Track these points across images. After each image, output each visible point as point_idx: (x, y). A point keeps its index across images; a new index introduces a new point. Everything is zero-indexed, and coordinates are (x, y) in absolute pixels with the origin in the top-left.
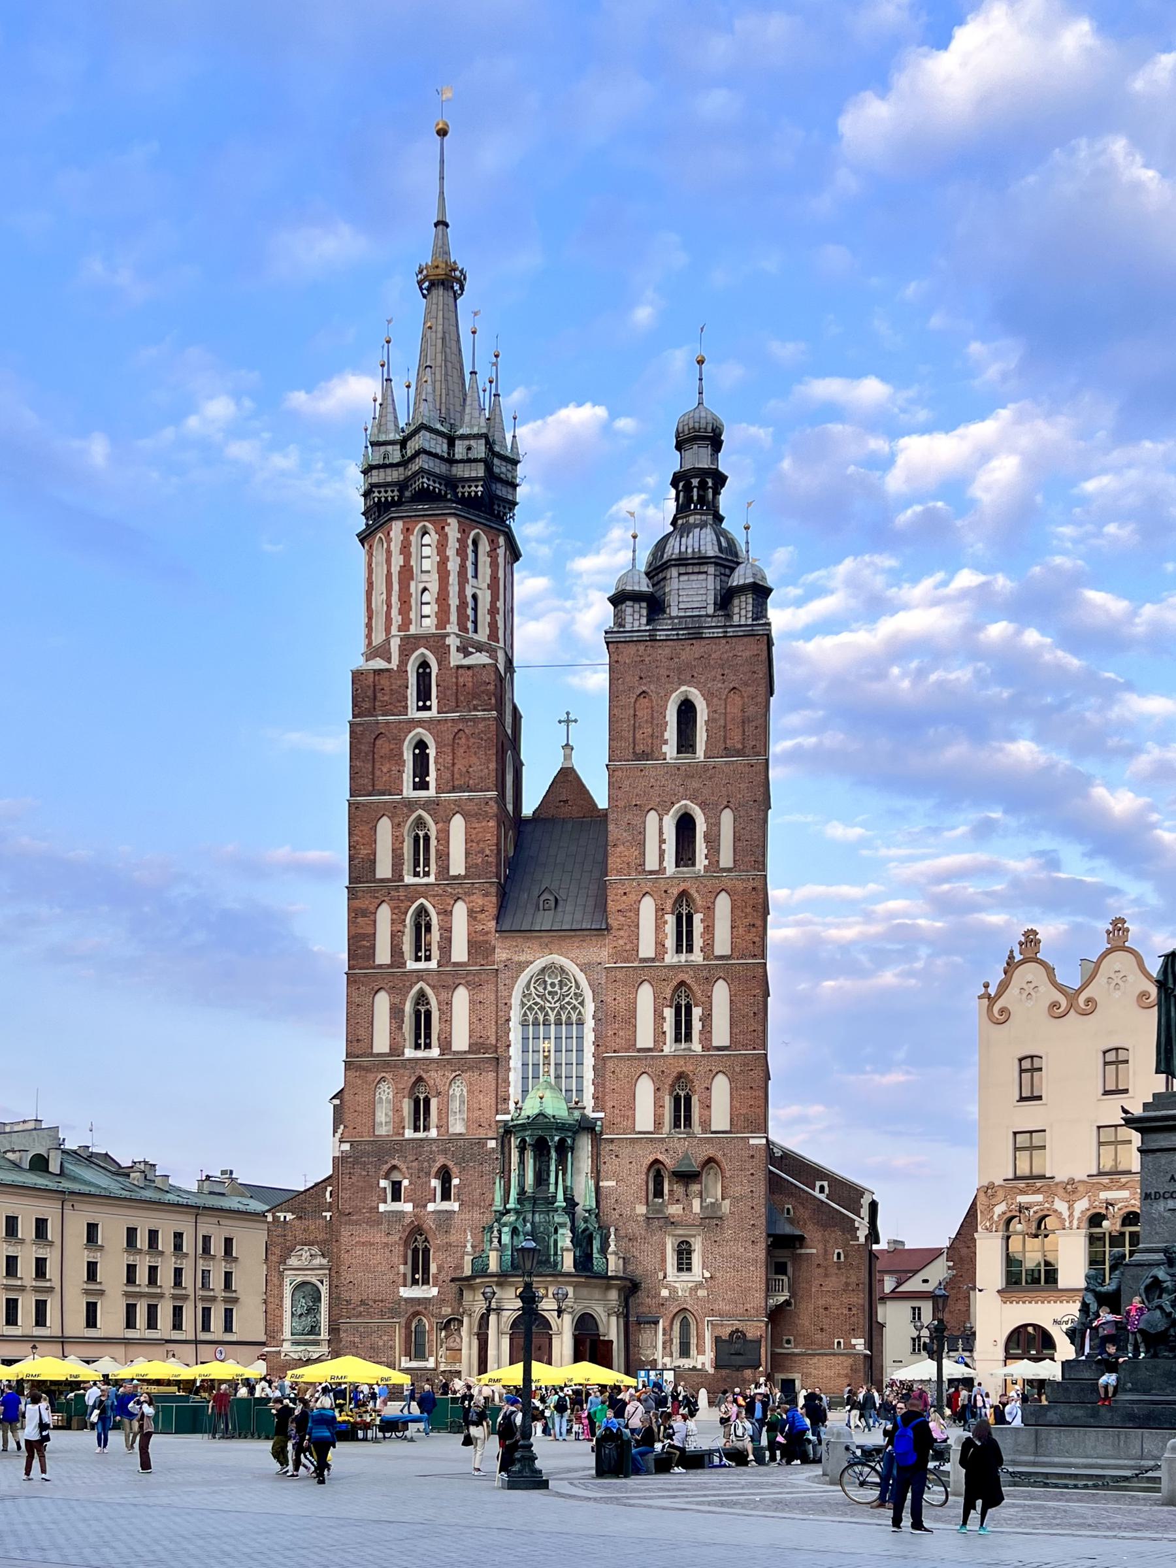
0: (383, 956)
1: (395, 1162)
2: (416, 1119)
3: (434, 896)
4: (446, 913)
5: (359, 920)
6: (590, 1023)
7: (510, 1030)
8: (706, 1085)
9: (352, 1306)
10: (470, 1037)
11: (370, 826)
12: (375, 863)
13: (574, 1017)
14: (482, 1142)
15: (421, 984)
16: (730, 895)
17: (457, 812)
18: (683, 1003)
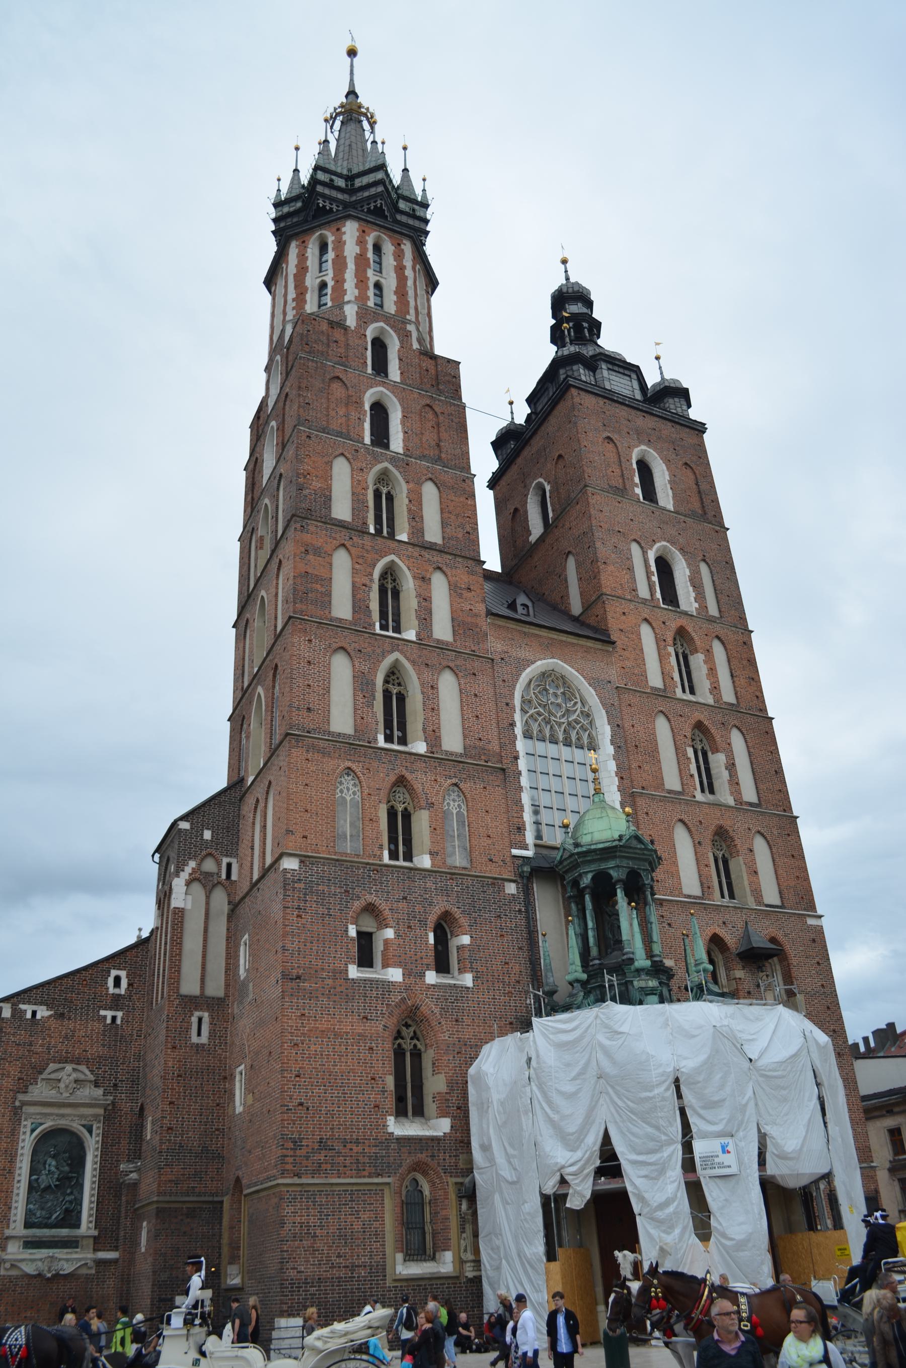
0: (342, 608)
1: (371, 898)
2: (393, 840)
3: (408, 557)
4: (424, 580)
5: (310, 557)
6: (607, 749)
7: (515, 737)
8: (747, 846)
9: (303, 1152)
10: (465, 737)
11: (326, 459)
12: (330, 500)
13: (585, 740)
14: (497, 883)
15: (396, 655)
16: (723, 643)
17: (431, 479)
18: (699, 747)
